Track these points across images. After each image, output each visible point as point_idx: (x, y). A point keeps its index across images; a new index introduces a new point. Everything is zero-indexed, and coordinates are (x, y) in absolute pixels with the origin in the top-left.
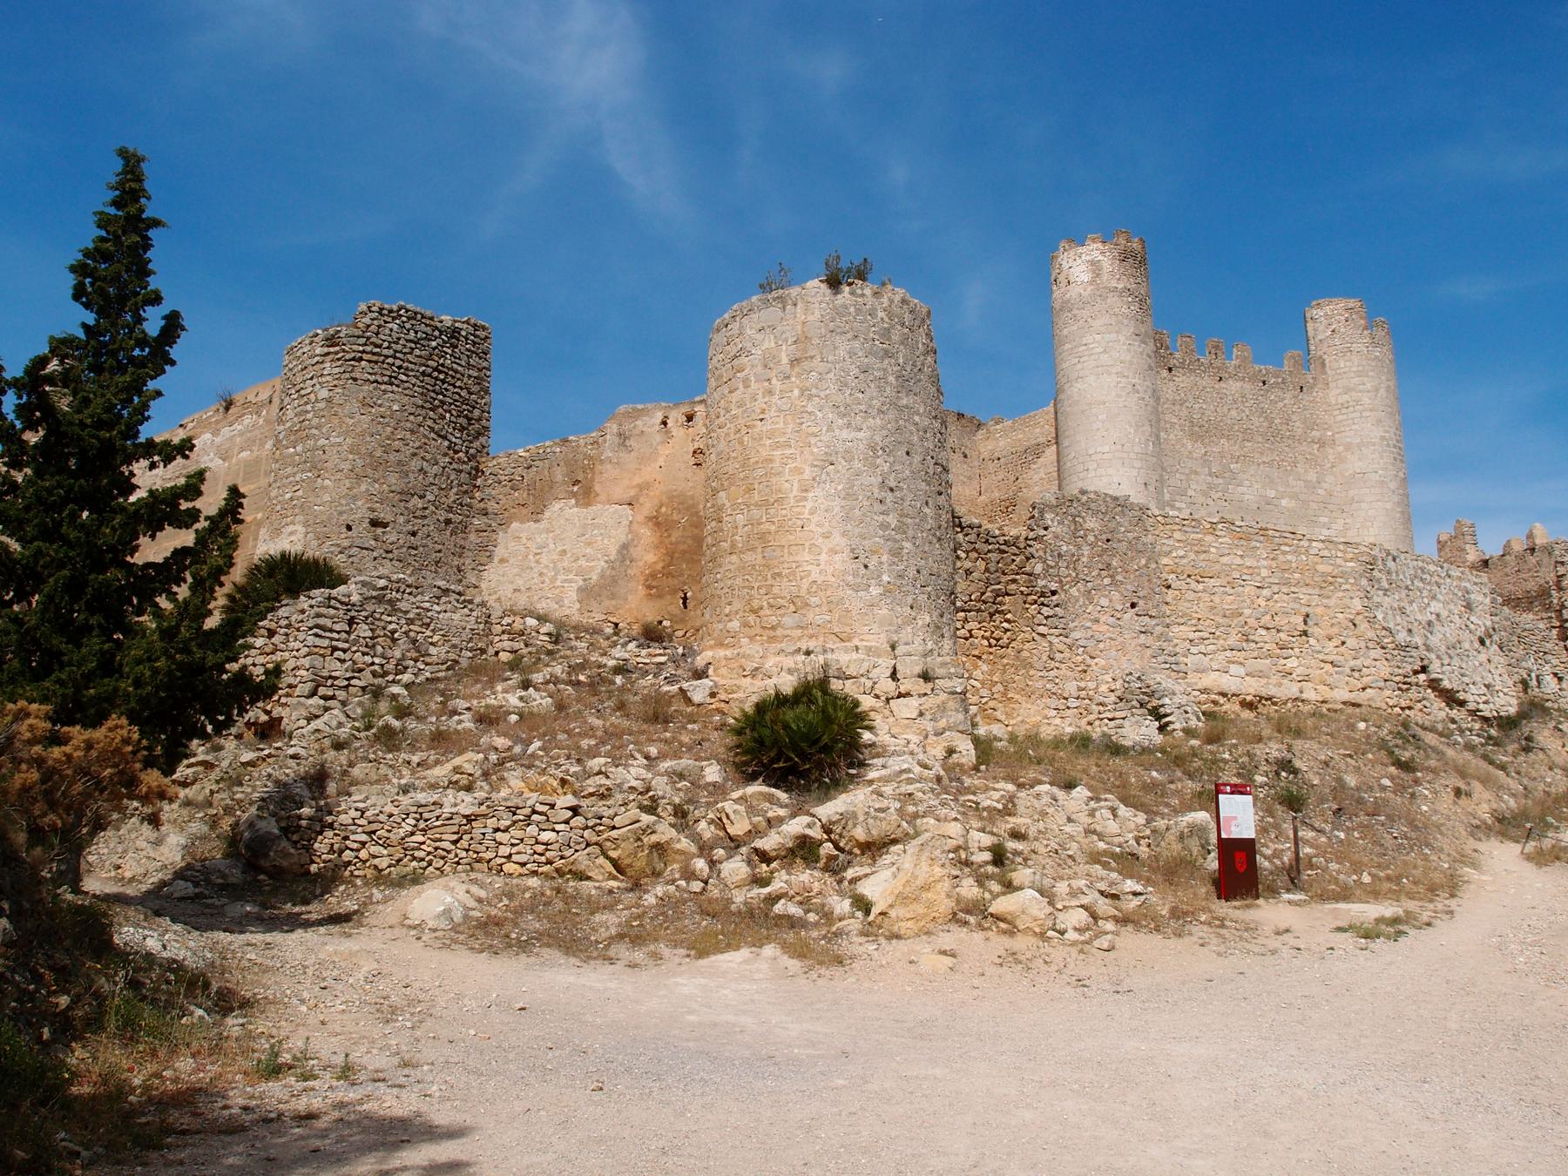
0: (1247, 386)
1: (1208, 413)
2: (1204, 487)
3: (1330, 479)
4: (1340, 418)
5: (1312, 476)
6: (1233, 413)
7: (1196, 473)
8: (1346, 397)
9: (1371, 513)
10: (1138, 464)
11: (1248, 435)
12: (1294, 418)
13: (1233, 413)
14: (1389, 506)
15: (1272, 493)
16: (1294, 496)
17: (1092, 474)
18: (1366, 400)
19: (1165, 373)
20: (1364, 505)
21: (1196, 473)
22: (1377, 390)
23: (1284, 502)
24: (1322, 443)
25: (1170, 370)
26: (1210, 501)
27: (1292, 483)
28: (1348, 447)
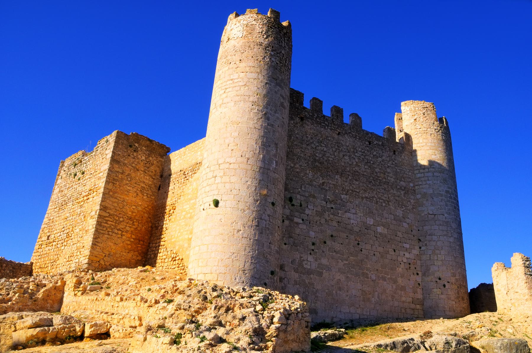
3: (411, 216)
4: (419, 175)
6: (347, 158)
7: (314, 197)
12: (389, 170)
13: (347, 158)
14: (451, 240)
15: (370, 221)
16: (386, 226)
17: (218, 180)
19: (298, 120)
20: (435, 238)
21: (314, 197)
24: (407, 191)
25: (302, 119)
27: (386, 215)
28: (424, 195)
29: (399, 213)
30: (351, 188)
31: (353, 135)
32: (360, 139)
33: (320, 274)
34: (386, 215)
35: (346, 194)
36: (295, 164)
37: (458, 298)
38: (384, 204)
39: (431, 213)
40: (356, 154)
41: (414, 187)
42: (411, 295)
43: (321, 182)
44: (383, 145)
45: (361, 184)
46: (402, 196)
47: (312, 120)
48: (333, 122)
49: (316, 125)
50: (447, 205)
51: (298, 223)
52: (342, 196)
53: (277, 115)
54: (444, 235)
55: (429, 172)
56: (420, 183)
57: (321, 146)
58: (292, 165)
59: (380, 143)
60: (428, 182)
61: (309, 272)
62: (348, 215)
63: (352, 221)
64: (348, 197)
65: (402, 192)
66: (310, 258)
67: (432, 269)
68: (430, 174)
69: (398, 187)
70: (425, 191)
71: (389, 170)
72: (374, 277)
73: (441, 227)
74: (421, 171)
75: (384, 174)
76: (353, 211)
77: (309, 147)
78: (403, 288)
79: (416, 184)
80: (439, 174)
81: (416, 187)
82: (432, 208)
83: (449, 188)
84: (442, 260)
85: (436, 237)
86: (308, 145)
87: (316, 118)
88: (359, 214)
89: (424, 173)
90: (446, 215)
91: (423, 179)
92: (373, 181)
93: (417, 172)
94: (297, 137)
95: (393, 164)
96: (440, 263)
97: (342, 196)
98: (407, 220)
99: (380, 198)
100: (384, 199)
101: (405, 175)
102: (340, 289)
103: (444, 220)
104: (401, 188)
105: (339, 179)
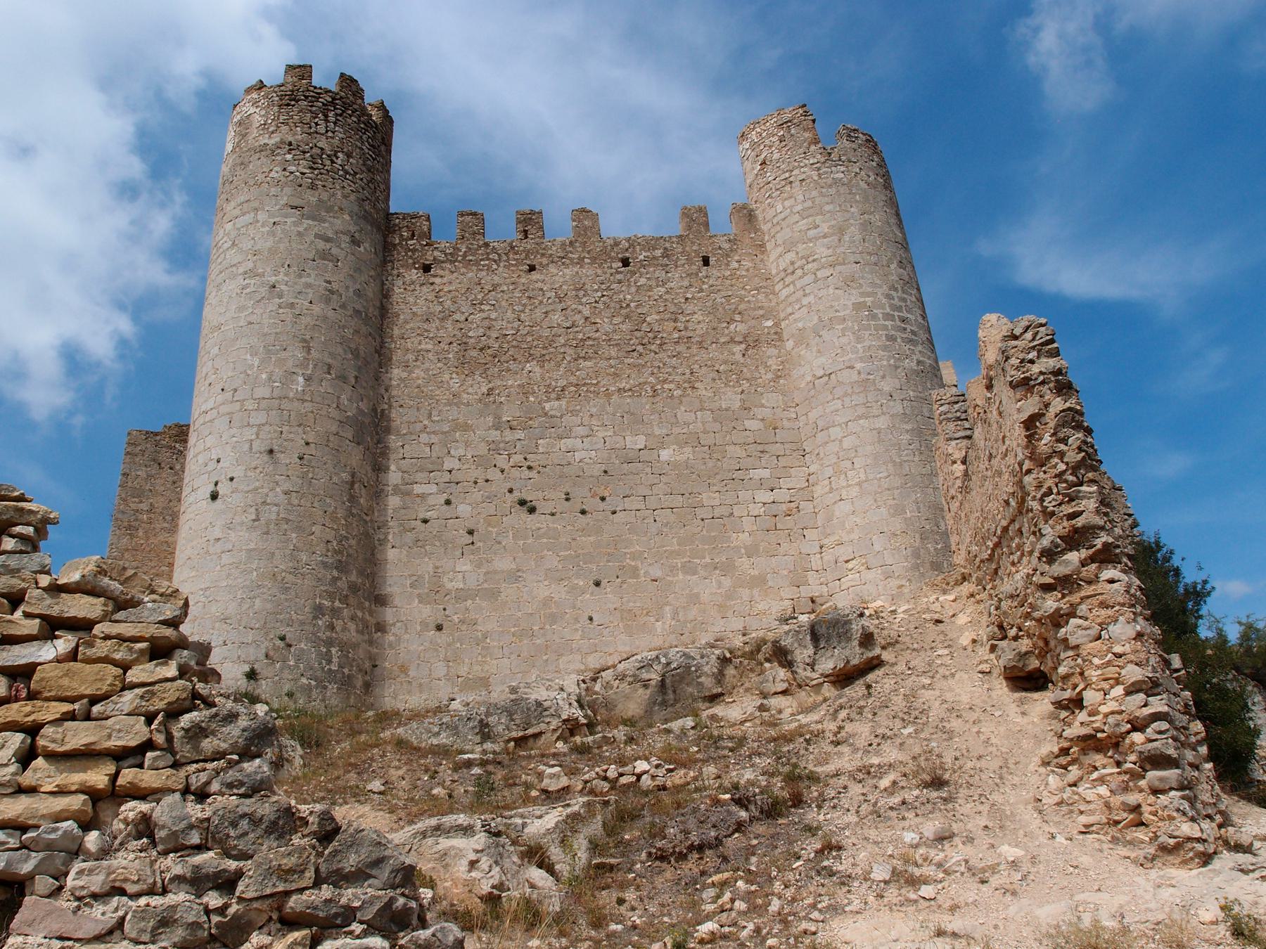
0: (588, 271)
1: (498, 324)
2: (483, 449)
5: (731, 399)
6: (557, 318)
7: (466, 428)
8: (791, 256)
9: (847, 443)
10: (260, 418)
11: (584, 348)
13: (557, 318)
18: (822, 251)
20: (835, 432)
21: (466, 428)
22: (841, 231)
23: (665, 454)
25: (427, 269)
26: (494, 474)
29: (731, 399)
30: (573, 379)
31: (571, 259)
32: (593, 260)
33: (493, 594)
34: (690, 417)
35: (558, 399)
36: (410, 372)
37: (916, 567)
38: (677, 393)
39: (821, 373)
40: (584, 300)
41: (776, 325)
42: (788, 592)
43: (484, 390)
44: (666, 254)
45: (603, 364)
46: (739, 357)
47: (452, 262)
48: (512, 248)
49: (463, 270)
50: (859, 340)
51: (423, 497)
52: (547, 406)
53: (303, 280)
54: (860, 417)
55: (805, 274)
56: (789, 310)
57: (482, 311)
58: (405, 375)
59: (658, 253)
60: (805, 301)
61: (462, 595)
62: (566, 443)
63: (578, 456)
64: (563, 403)
65: (738, 349)
66: (464, 566)
67: (837, 513)
68: (809, 279)
69: (722, 340)
70: (800, 325)
71: (689, 308)
72: (657, 572)
73: (847, 400)
74: (789, 280)
75: (675, 321)
76: (581, 431)
77: (449, 324)
78: (759, 581)
79: (782, 315)
80: (827, 272)
81: (783, 325)
82: (823, 359)
83: (862, 294)
84: (859, 484)
85: (838, 429)
86: (442, 319)
87: (465, 255)
88: (600, 435)
89: (793, 282)
90: (858, 366)
91: (791, 299)
92: (640, 348)
93: (780, 285)
94: (414, 314)
95: (701, 290)
96: (855, 491)
97: (547, 406)
98: (760, 413)
99: (665, 381)
100: (678, 378)
101: (742, 307)
102: (553, 618)
103: (855, 377)
104: (732, 341)
105: (537, 369)
